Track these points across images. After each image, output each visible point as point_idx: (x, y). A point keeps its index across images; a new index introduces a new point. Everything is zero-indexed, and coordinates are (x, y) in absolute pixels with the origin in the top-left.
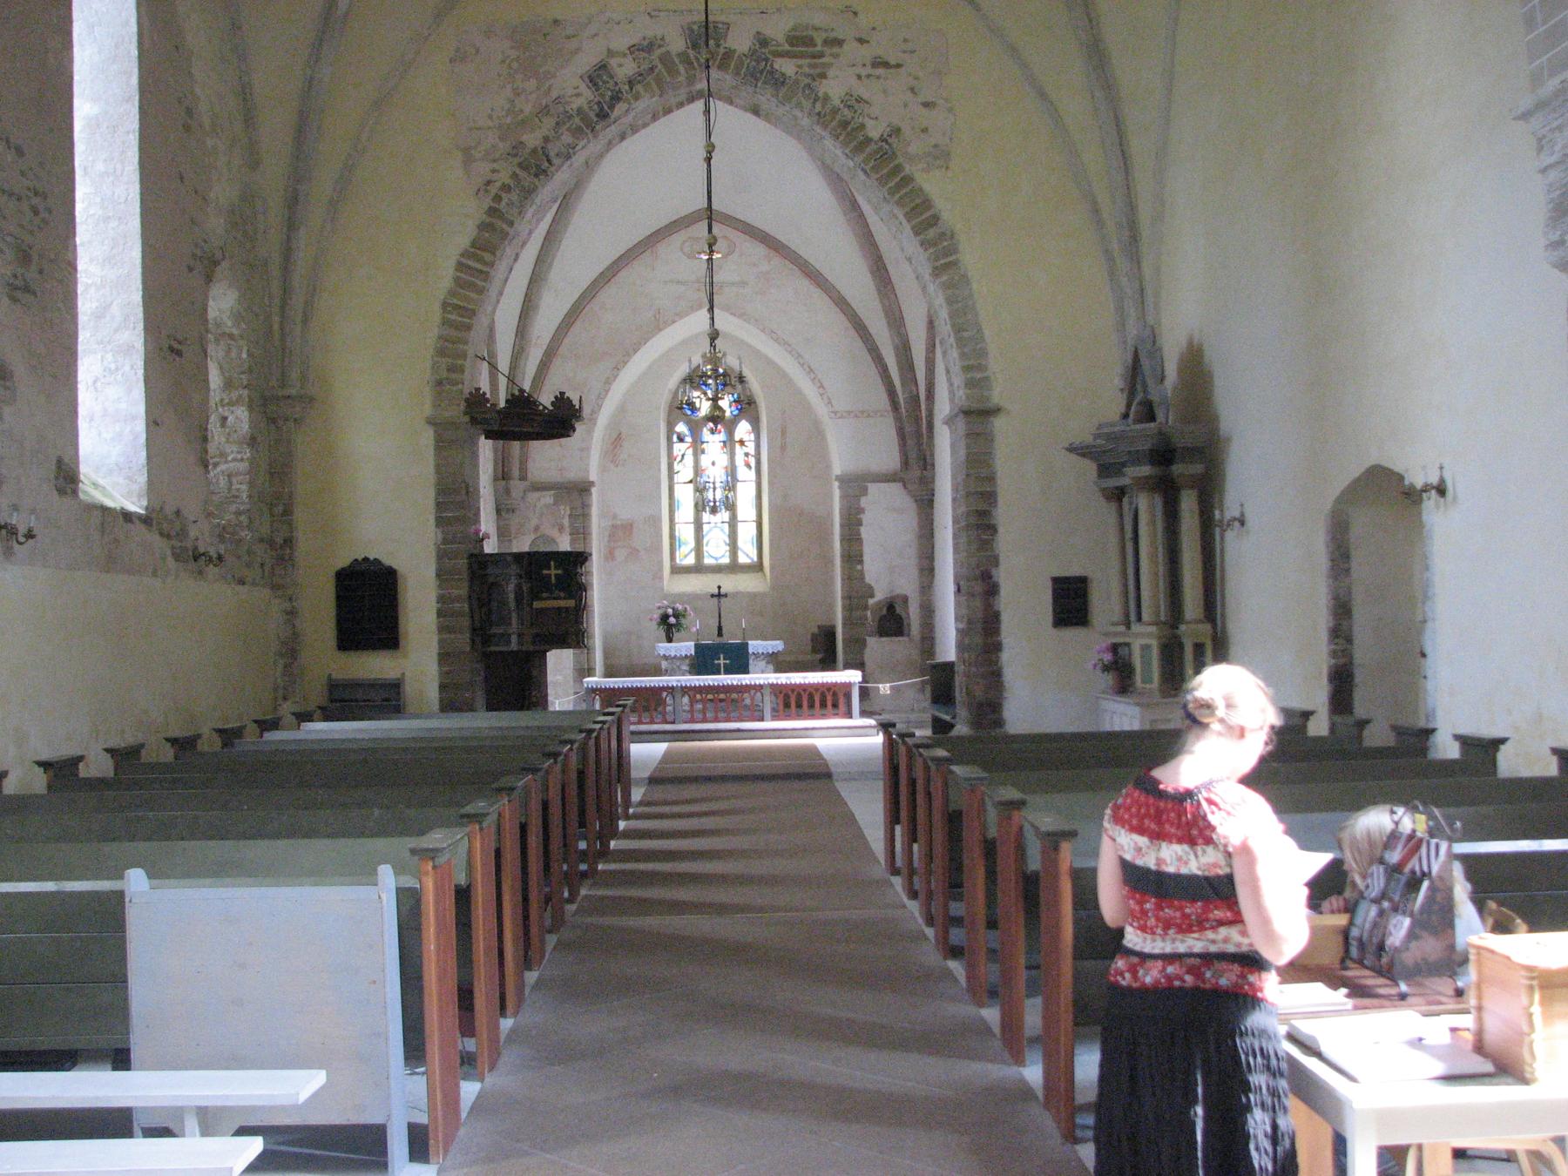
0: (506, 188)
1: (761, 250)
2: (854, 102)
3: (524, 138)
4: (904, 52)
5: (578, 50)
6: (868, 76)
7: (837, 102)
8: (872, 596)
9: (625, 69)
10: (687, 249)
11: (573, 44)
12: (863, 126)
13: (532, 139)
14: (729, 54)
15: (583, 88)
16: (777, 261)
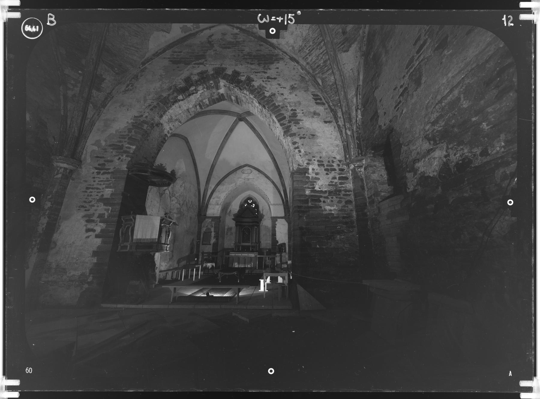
0: (155, 107)
1: (256, 172)
2: (261, 88)
3: (163, 94)
4: (277, 75)
5: (182, 74)
6: (266, 81)
7: (256, 87)
8: (278, 243)
9: (195, 78)
10: (243, 172)
11: (181, 72)
12: (264, 93)
13: (165, 95)
14: (226, 74)
15: (182, 83)
16: (261, 174)
